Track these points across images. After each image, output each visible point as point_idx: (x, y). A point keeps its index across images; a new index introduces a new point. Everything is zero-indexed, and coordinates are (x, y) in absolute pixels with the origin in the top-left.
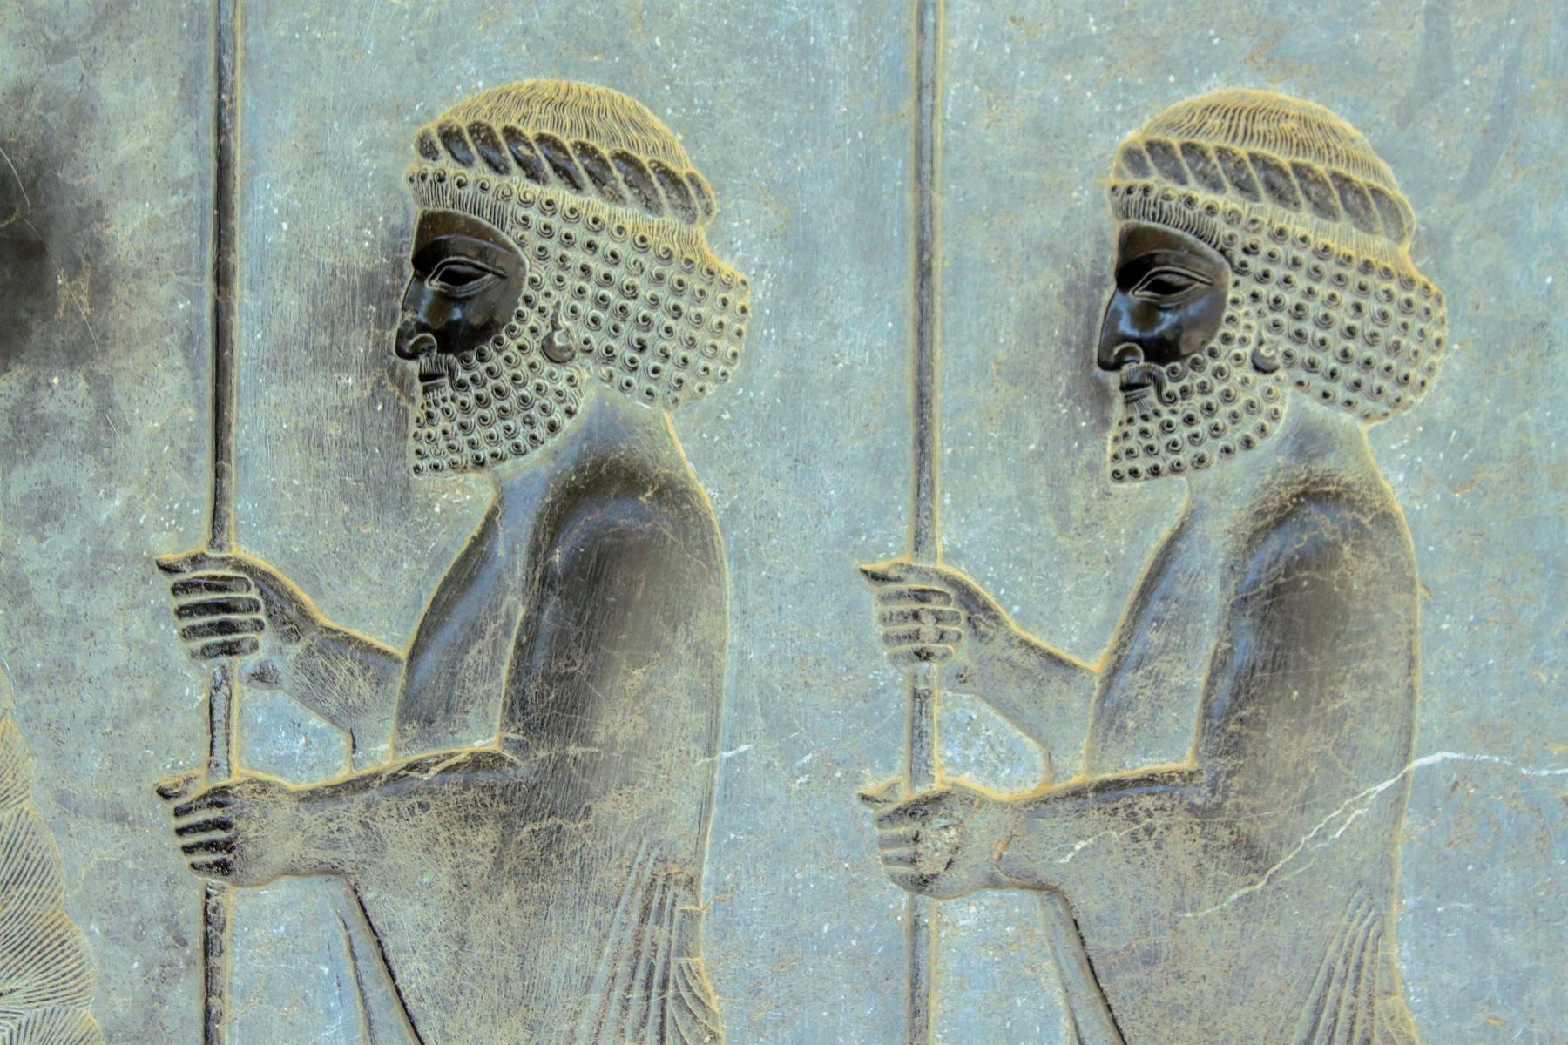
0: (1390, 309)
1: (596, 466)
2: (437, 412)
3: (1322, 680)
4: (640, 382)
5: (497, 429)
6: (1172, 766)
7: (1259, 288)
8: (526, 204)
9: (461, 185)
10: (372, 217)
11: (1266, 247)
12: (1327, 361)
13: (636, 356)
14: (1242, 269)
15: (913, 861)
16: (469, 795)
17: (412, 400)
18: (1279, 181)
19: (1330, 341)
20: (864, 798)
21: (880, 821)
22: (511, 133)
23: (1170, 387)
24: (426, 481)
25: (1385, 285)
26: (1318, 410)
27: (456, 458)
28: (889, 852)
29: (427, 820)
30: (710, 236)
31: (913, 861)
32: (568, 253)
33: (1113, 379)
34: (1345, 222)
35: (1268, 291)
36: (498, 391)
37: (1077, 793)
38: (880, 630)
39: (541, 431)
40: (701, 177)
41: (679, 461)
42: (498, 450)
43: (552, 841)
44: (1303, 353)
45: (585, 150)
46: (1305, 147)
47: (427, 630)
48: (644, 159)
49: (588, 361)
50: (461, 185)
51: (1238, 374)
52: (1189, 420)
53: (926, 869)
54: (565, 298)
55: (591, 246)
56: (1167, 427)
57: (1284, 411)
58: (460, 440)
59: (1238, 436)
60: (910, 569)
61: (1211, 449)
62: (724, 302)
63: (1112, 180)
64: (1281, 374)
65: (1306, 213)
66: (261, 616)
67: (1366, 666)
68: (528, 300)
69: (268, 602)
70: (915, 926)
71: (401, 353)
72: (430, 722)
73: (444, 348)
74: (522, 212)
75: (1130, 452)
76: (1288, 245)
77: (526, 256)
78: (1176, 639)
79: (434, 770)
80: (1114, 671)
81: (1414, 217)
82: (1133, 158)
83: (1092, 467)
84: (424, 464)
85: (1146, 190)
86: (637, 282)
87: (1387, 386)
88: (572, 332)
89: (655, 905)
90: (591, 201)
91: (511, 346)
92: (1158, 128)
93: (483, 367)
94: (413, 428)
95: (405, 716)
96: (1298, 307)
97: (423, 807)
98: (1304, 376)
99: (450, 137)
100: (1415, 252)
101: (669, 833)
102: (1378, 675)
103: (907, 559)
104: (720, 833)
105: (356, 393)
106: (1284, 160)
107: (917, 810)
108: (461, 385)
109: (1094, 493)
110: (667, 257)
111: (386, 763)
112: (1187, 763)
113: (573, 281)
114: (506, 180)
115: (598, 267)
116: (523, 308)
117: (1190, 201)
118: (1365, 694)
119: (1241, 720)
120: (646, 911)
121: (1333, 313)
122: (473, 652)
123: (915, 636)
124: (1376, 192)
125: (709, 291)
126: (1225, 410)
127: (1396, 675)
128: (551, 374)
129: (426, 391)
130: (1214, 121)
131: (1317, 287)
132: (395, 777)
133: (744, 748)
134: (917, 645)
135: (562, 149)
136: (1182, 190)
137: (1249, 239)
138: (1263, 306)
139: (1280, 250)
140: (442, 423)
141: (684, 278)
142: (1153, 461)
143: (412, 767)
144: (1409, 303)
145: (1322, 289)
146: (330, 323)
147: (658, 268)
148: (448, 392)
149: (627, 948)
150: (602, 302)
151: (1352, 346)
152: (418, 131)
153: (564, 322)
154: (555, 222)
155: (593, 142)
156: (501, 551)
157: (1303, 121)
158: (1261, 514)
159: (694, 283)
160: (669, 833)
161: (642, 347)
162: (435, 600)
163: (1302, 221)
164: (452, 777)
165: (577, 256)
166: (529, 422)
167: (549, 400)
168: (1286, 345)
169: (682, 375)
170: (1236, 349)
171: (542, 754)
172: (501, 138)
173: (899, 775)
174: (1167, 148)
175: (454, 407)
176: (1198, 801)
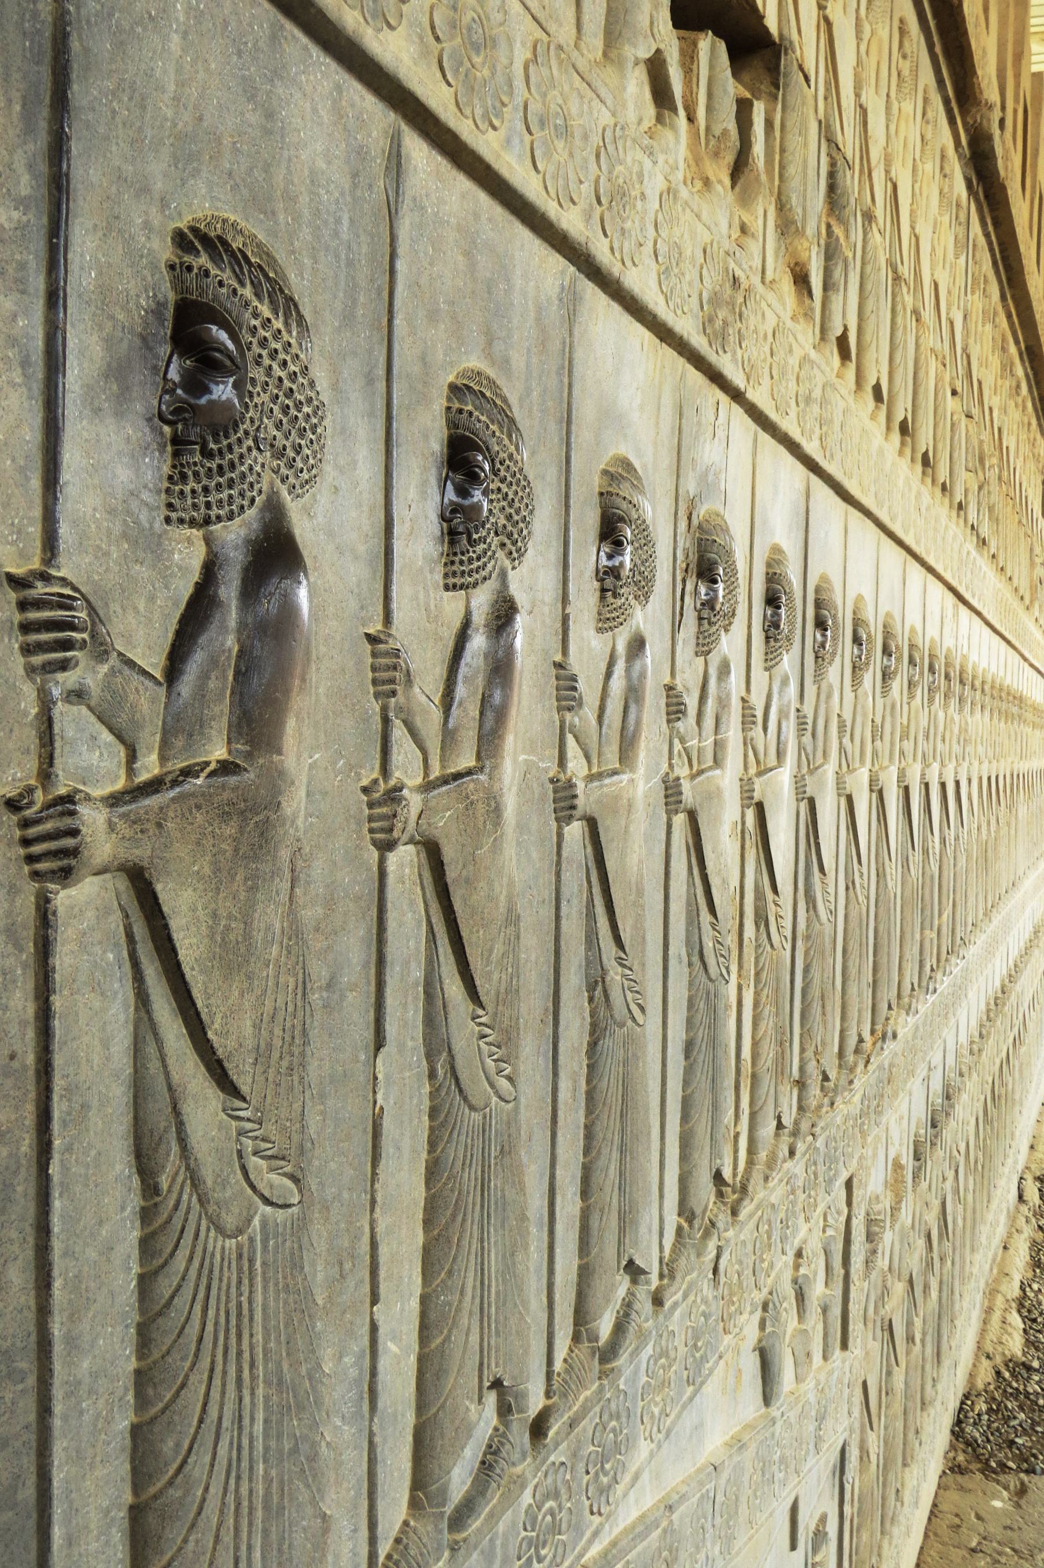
5: (224, 495)
8: (256, 315)
23: (475, 536)
28: (374, 825)
31: (391, 830)
35: (504, 488)
39: (246, 503)
54: (265, 397)
71: (161, 418)
74: (253, 322)
75: (454, 574)
84: (174, 515)
85: (471, 414)
97: (198, 807)
99: (205, 239)
103: (380, 627)
111: (156, 771)
133: (317, 756)
137: (502, 455)
140: (192, 484)
148: (198, 458)
153: (265, 420)
158: (498, 617)
173: (375, 775)
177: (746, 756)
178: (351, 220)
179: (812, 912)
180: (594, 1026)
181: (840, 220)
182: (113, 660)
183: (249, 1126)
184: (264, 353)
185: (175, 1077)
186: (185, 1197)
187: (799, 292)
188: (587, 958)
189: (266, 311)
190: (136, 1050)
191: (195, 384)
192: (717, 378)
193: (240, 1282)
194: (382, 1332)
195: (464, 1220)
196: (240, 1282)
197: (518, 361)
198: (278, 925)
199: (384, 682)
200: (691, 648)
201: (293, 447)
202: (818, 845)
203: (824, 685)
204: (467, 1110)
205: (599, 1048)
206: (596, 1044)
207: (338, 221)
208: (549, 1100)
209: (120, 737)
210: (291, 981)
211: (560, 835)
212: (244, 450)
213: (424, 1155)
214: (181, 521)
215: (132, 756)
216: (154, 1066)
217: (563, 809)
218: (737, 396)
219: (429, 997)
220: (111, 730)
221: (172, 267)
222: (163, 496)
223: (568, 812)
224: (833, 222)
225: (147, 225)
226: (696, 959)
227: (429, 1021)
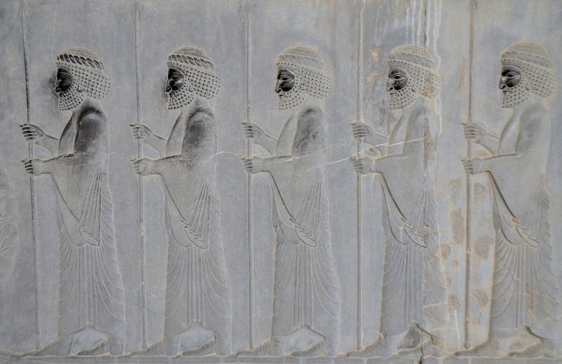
0: (210, 81)
1: (86, 108)
2: (62, 101)
3: (200, 140)
6: (178, 154)
7: (189, 78)
8: (73, 67)
9: (62, 64)
10: (51, 70)
12: (200, 89)
13: (92, 91)
14: (186, 75)
15: (138, 170)
16: (68, 160)
17: (59, 99)
18: (191, 61)
19: (200, 86)
20: (131, 160)
21: (134, 164)
22: (70, 56)
23: (176, 94)
24: (61, 111)
25: (209, 77)
27: (65, 108)
29: (62, 164)
30: (104, 72)
31: (138, 170)
32: (80, 74)
33: (168, 93)
34: (203, 67)
35: (190, 78)
36: (70, 97)
37: (163, 159)
39: (78, 103)
40: (102, 62)
41: (101, 108)
42: (72, 106)
43: (81, 167)
45: (82, 58)
46: (196, 55)
47: (63, 135)
48: (92, 59)
49: (85, 92)
50: (62, 64)
51: (186, 92)
52: (179, 99)
53: (140, 171)
57: (195, 98)
58: (66, 105)
59: (187, 102)
60: (137, 124)
61: (183, 104)
62: (106, 82)
63: (167, 61)
64: (194, 92)
65: (196, 65)
66: (36, 133)
67: (208, 138)
68: (74, 82)
69: (37, 131)
71: (56, 91)
72: (63, 149)
73: (62, 90)
74: (72, 68)
76: (193, 71)
77: (73, 75)
78: (178, 134)
79: (63, 157)
80: (169, 140)
81: (215, 66)
83: (165, 107)
84: (61, 109)
86: (91, 79)
87: (211, 93)
88: (81, 87)
89: (99, 177)
90: (83, 66)
91: (72, 90)
92: (174, 53)
93: (68, 93)
94: (59, 103)
95: (59, 149)
96: (195, 81)
98: (197, 92)
100: (216, 72)
101: (101, 166)
102: (210, 139)
103: (136, 123)
104: (110, 166)
105: (50, 98)
106: (193, 57)
107: (138, 162)
108: (64, 96)
109: (166, 112)
112: (180, 154)
113: (81, 79)
114: (69, 63)
115: (85, 77)
116: (73, 84)
117: (177, 64)
118: (208, 142)
119: (187, 147)
120: (97, 179)
121: (201, 82)
122: (69, 138)
124: (208, 62)
125: (103, 80)
126: (185, 98)
127: (213, 139)
128: (79, 94)
129: (61, 97)
130: (182, 51)
131: (198, 78)
132: (57, 158)
134: (138, 136)
135: (78, 58)
136: (177, 62)
137: (186, 70)
138: (190, 81)
139: (192, 72)
141: (99, 78)
142: (174, 106)
143: (60, 157)
144: (213, 80)
145: (199, 78)
146: (45, 87)
147: (94, 77)
148: (63, 97)
149: (94, 184)
150: (86, 82)
151: (204, 87)
152: (57, 55)
153: (80, 86)
154: (77, 70)
155: (83, 57)
156: (73, 122)
157: (197, 51)
159: (100, 79)
160: (101, 166)
163: (195, 67)
164: (65, 158)
165: (81, 75)
166: (76, 102)
167: (79, 98)
168: (194, 87)
169: (100, 94)
170: (186, 88)
171: (79, 154)
172: (68, 56)
173: (137, 157)
174: (174, 56)
175: (64, 100)
176: (181, 160)
183: (81, 225)
184: (77, 73)
186: (65, 235)
204: (179, 245)
208: (248, 257)
210: (95, 200)
211: (249, 177)
223: (250, 169)
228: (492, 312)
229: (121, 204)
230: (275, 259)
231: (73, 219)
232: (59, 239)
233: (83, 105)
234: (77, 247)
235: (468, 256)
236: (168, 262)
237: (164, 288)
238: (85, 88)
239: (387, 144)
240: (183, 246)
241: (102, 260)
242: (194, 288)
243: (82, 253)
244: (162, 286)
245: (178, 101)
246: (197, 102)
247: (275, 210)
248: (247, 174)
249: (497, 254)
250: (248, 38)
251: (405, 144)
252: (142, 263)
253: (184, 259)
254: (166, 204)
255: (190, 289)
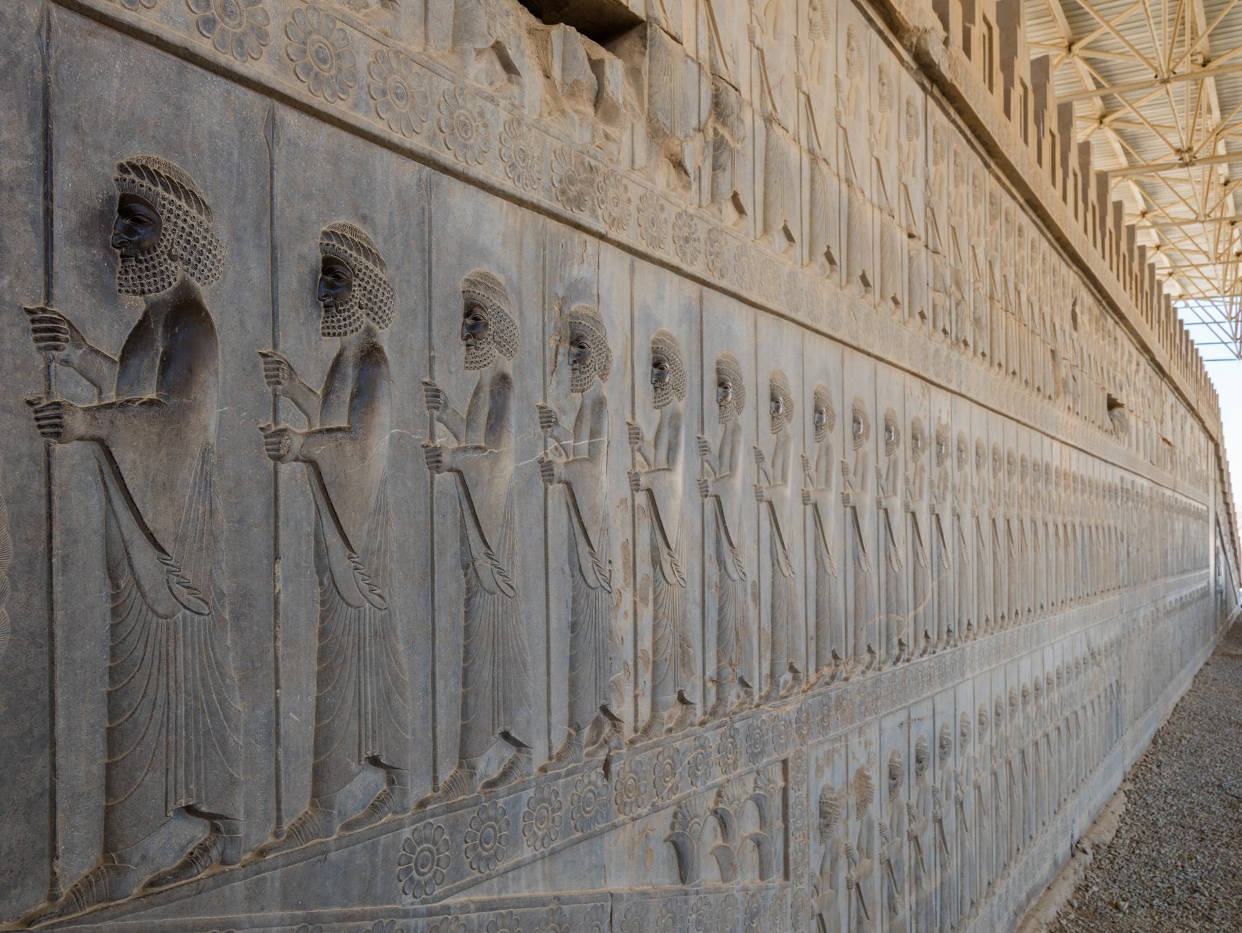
4: (197, 275)
5: (152, 280)
8: (164, 199)
11: (364, 270)
12: (376, 309)
14: (357, 276)
20: (261, 429)
24: (123, 296)
26: (373, 324)
28: (269, 447)
35: (364, 284)
36: (154, 267)
38: (264, 373)
39: (166, 284)
44: (370, 305)
52: (345, 320)
53: (282, 452)
54: (175, 236)
55: (185, 220)
56: (339, 321)
58: (138, 282)
61: (349, 329)
70: (276, 473)
79: (137, 403)
82: (325, 234)
84: (123, 289)
85: (334, 245)
88: (178, 251)
99: (134, 167)
108: (140, 262)
110: (207, 230)
111: (114, 400)
112: (344, 424)
115: (188, 230)
123: (277, 376)
129: (123, 262)
132: (121, 405)
137: (359, 267)
140: (131, 275)
148: (134, 263)
150: (188, 242)
161: (199, 261)
162: (128, 341)
166: (163, 280)
177: (633, 459)
178: (240, 153)
179: (723, 571)
180: (468, 590)
181: (724, 124)
182: (85, 348)
183: (173, 569)
184: (172, 216)
185: (126, 537)
187: (678, 174)
188: (461, 550)
189: (172, 197)
190: (106, 522)
191: (130, 231)
192: (578, 226)
193: (168, 640)
194: (282, 705)
195: (344, 662)
196: (168, 640)
197: (381, 219)
198: (191, 481)
199: (272, 377)
200: (566, 387)
201: (196, 259)
202: (726, 528)
203: (730, 425)
204: (345, 605)
205: (472, 602)
206: (469, 599)
207: (231, 154)
208: (430, 623)
209: (93, 383)
211: (432, 478)
212: (162, 260)
213: (318, 625)
214: (127, 291)
215: (101, 393)
216: (114, 531)
217: (432, 462)
218: (602, 237)
219: (317, 542)
220: (88, 379)
221: (117, 180)
222: (117, 280)
224: (719, 127)
225: (101, 163)
226: (577, 573)
227: (318, 555)
228: (653, 680)
229: (239, 522)
230: (463, 624)
231: (152, 553)
232: (109, 605)
233: (177, 290)
234: (160, 620)
235: (635, 603)
236: (320, 642)
237: (312, 700)
238: (185, 254)
239: (571, 442)
240: (351, 606)
241: (213, 649)
242: (369, 688)
243: (172, 634)
244: (308, 695)
245: (343, 323)
246: (369, 331)
247: (464, 539)
248: (428, 472)
249: (655, 599)
250: (430, 236)
251: (590, 444)
252: (276, 648)
253: (352, 632)
254: (317, 524)
255: (363, 690)
